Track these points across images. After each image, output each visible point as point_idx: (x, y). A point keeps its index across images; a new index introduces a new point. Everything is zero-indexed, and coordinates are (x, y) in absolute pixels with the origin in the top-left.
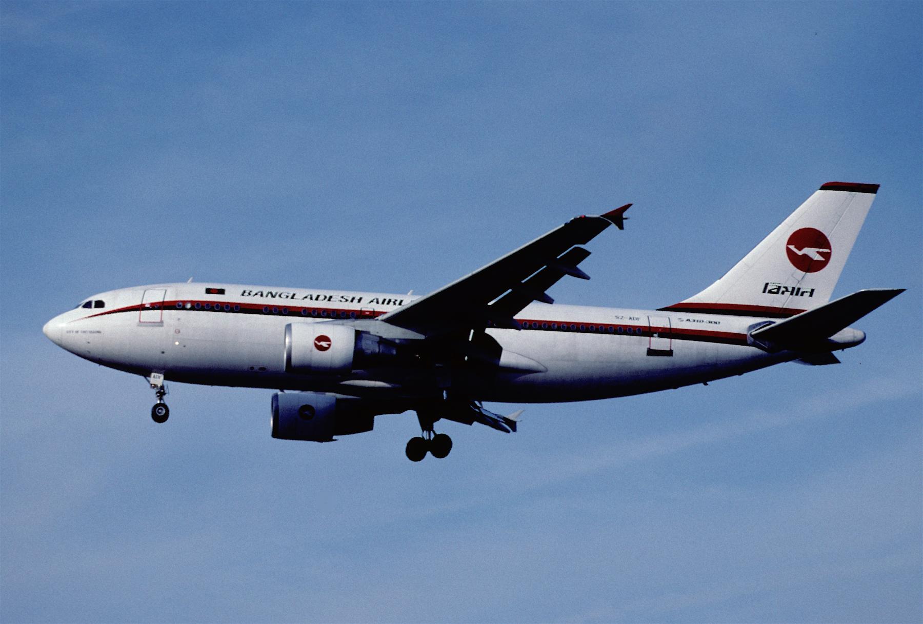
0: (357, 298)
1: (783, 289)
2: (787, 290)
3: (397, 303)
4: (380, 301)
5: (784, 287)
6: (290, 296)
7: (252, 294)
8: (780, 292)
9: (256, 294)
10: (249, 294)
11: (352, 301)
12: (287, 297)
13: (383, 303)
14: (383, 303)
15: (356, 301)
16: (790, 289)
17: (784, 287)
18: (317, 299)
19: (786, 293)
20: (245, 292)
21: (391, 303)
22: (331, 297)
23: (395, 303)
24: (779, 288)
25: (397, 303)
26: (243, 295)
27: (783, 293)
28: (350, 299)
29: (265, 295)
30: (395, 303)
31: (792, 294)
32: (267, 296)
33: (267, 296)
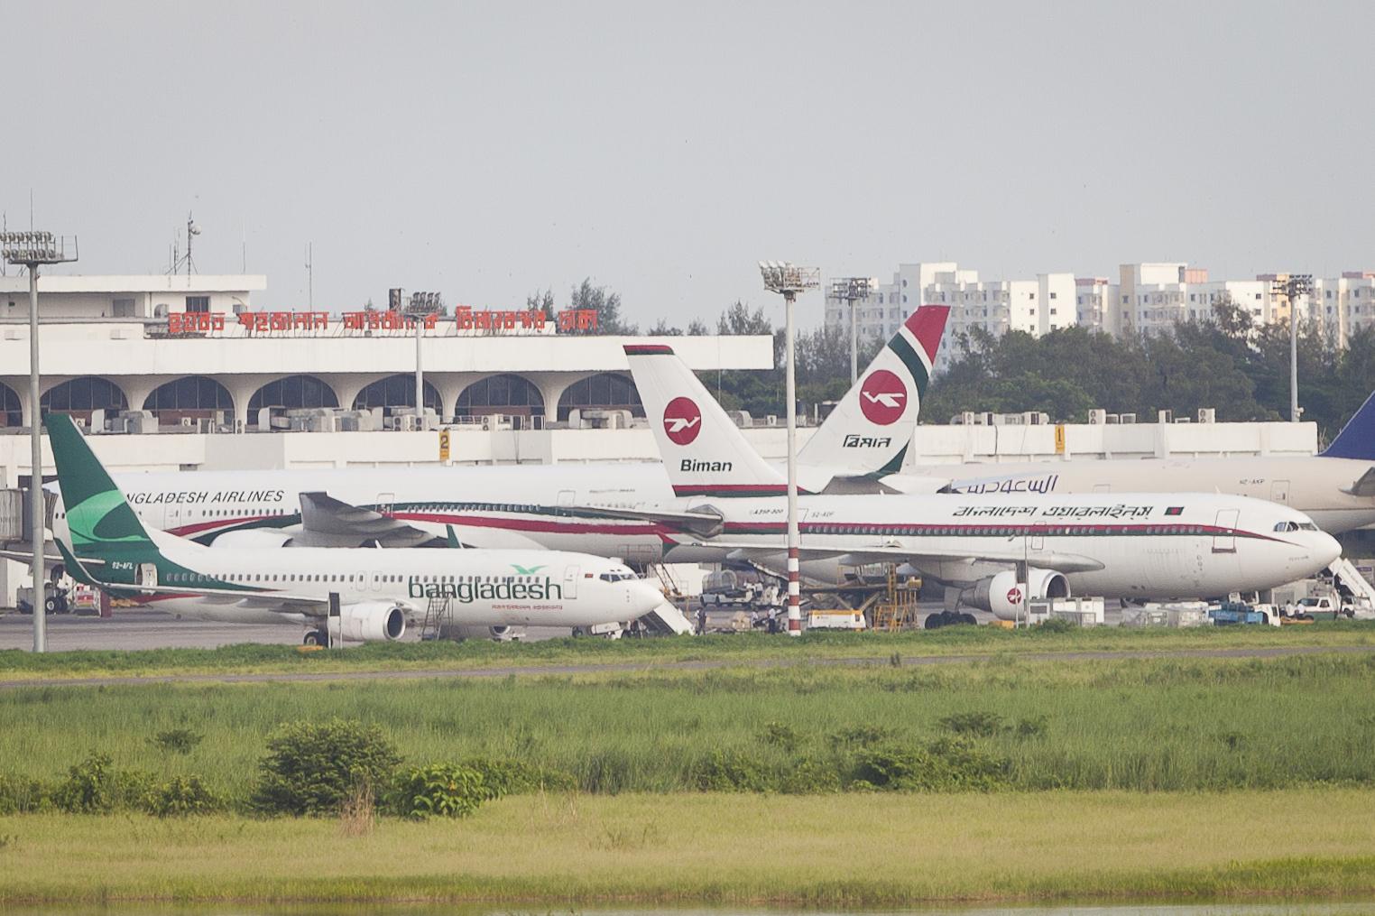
0: (203, 495)
1: (861, 441)
2: (865, 442)
5: (865, 440)
8: (859, 444)
12: (143, 500)
15: (201, 499)
21: (232, 499)
24: (858, 440)
25: (238, 498)
27: (861, 446)
31: (869, 446)
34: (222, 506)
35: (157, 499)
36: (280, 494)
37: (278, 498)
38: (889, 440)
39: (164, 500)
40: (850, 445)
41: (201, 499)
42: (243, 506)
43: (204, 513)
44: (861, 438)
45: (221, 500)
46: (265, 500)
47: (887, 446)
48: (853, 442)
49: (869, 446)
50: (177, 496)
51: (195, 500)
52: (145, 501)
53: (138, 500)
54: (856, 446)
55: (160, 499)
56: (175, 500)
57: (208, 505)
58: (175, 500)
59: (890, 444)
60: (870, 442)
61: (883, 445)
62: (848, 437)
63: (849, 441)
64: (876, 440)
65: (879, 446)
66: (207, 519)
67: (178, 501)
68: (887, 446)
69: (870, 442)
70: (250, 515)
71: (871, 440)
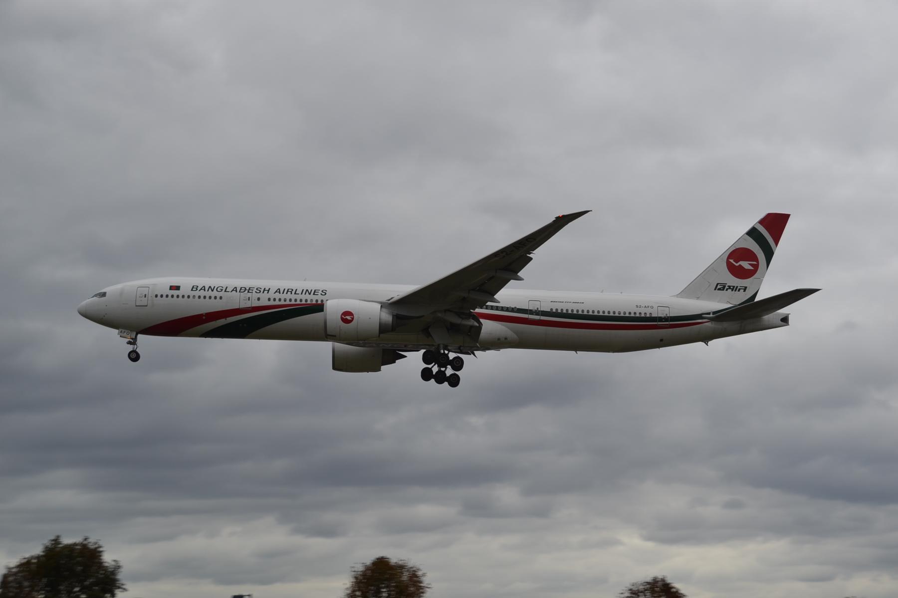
0: (267, 289)
1: (727, 287)
2: (730, 289)
3: (293, 292)
4: (282, 292)
5: (728, 286)
7: (199, 289)
8: (725, 289)
9: (201, 289)
10: (197, 289)
11: (263, 292)
12: (222, 290)
13: (283, 293)
14: (283, 293)
15: (266, 292)
16: (732, 287)
17: (728, 286)
18: (240, 292)
19: (729, 290)
20: (193, 287)
21: (289, 293)
23: (291, 293)
24: (725, 286)
25: (293, 292)
26: (192, 290)
27: (727, 290)
28: (262, 291)
29: (206, 289)
30: (291, 293)
31: (732, 290)
32: (208, 291)
33: (208, 291)
34: (283, 296)
35: (233, 290)
38: (746, 288)
39: (238, 290)
40: (719, 289)
42: (299, 297)
43: (269, 299)
44: (727, 285)
45: (282, 292)
46: (314, 294)
47: (744, 291)
48: (721, 287)
49: (732, 290)
50: (248, 289)
51: (262, 291)
52: (224, 290)
53: (218, 290)
54: (723, 290)
55: (235, 289)
56: (247, 291)
57: (271, 295)
58: (247, 291)
59: (747, 290)
60: (733, 288)
62: (718, 284)
63: (719, 287)
64: (737, 287)
65: (739, 291)
66: (272, 303)
67: (248, 292)
68: (744, 291)
69: (733, 288)
70: (304, 302)
71: (734, 287)
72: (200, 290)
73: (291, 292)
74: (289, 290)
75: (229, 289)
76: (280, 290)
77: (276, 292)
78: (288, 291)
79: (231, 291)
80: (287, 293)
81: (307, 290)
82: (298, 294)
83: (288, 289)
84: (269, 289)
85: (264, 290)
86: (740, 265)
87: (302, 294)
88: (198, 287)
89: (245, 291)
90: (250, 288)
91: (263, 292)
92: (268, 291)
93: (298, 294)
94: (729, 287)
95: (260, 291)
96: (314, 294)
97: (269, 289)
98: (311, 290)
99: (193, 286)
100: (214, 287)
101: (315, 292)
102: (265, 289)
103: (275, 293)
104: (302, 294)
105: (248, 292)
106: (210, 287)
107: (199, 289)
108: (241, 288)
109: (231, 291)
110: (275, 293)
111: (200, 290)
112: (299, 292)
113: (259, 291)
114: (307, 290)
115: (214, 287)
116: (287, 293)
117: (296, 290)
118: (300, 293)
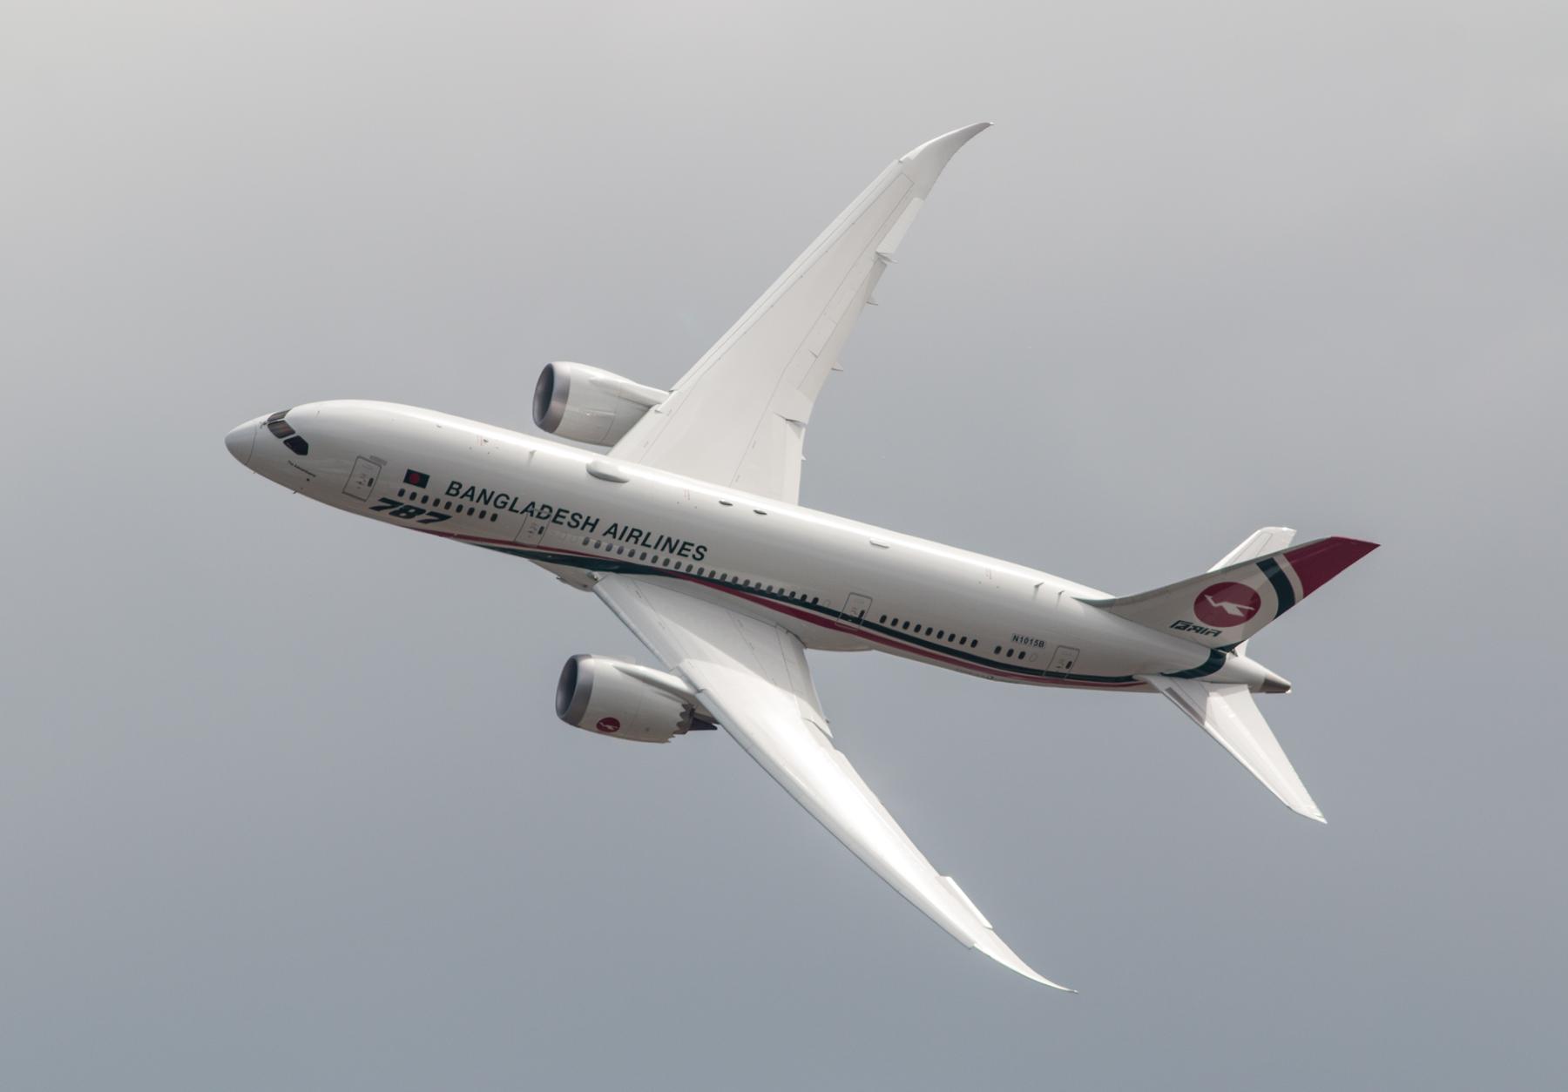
0: (592, 521)
1: (1191, 627)
3: (641, 540)
4: (618, 535)
6: (510, 502)
7: (462, 491)
9: (466, 494)
10: (458, 493)
11: (583, 528)
12: (505, 504)
13: (620, 539)
14: (620, 539)
15: (588, 528)
20: (451, 487)
22: (557, 515)
23: (636, 542)
25: (641, 540)
26: (448, 493)
27: (1189, 630)
28: (582, 522)
29: (476, 498)
30: (636, 542)
32: (478, 501)
33: (478, 501)
35: (526, 510)
36: (701, 550)
37: (698, 556)
39: (536, 514)
40: (1179, 628)
41: (588, 528)
45: (618, 535)
46: (679, 553)
52: (508, 506)
53: (499, 504)
61: (1211, 635)
63: (1179, 625)
69: (1197, 629)
71: (1201, 628)
72: (462, 497)
73: (637, 538)
74: (636, 534)
75: (519, 506)
76: (616, 530)
77: (608, 532)
78: (631, 535)
79: (522, 512)
80: (627, 540)
81: (669, 540)
82: (649, 546)
83: (633, 530)
84: (597, 520)
85: (587, 523)
86: (1221, 608)
87: (656, 547)
88: (460, 486)
89: (548, 516)
90: (560, 510)
91: (583, 528)
92: (594, 526)
93: (649, 546)
94: (1195, 628)
95: (578, 523)
96: (679, 553)
97: (597, 520)
98: (678, 541)
99: (453, 483)
100: (493, 493)
101: (683, 548)
102: (589, 518)
103: (605, 534)
104: (656, 547)
105: (554, 521)
106: (484, 492)
107: (462, 491)
108: (544, 507)
109: (522, 512)
110: (605, 534)
111: (462, 497)
112: (652, 541)
113: (574, 524)
114: (669, 540)
115: (493, 493)
116: (627, 540)
117: (649, 534)
118: (653, 545)
